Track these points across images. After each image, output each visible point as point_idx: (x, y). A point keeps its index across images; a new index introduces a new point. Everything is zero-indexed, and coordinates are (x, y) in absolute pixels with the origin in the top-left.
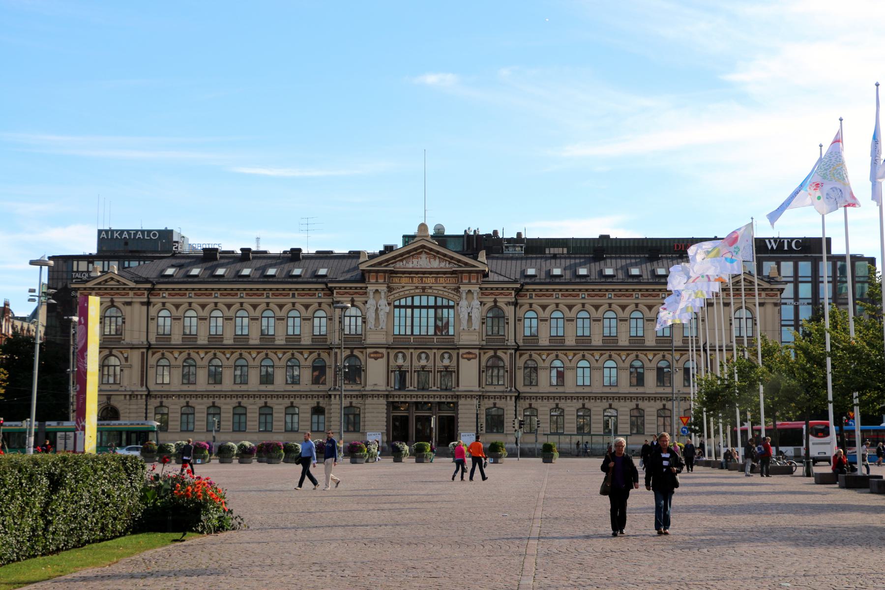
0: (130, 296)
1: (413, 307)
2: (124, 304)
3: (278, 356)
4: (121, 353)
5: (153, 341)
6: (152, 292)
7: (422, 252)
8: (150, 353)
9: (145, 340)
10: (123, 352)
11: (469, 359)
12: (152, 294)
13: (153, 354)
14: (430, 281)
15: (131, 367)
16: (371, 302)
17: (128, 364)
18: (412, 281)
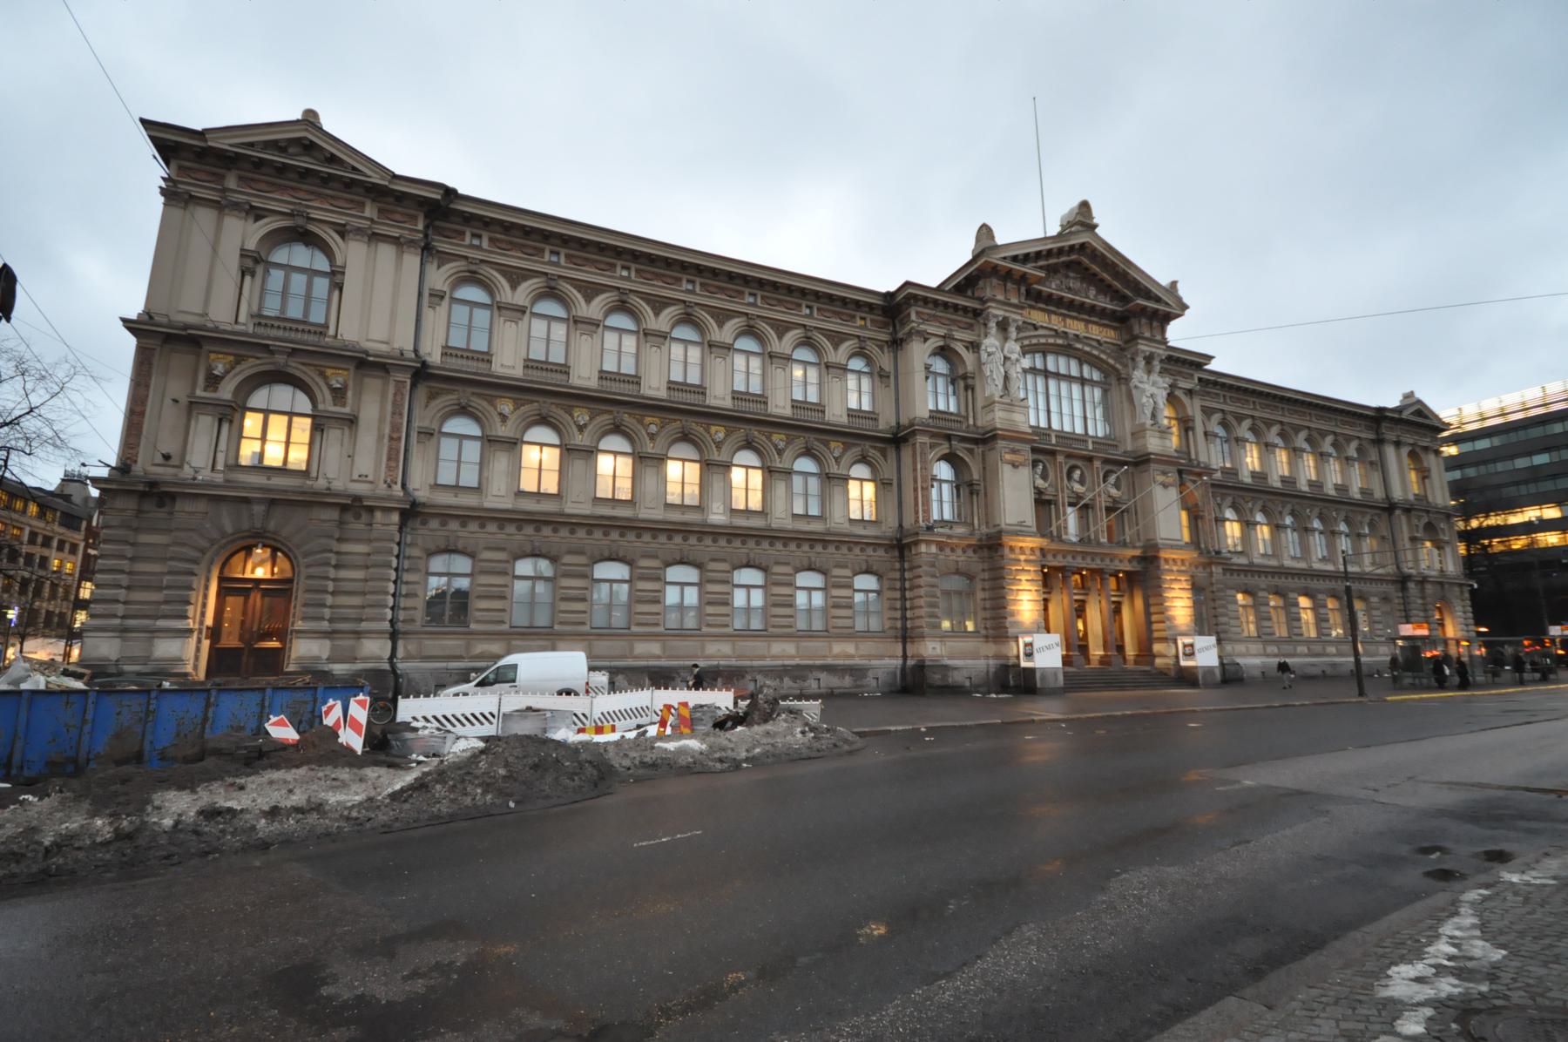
0: (367, 213)
1: (1046, 374)
2: (342, 235)
3: (776, 446)
4: (322, 374)
5: (434, 357)
6: (437, 223)
7: (1068, 266)
8: (422, 392)
9: (411, 348)
10: (329, 372)
11: (1165, 486)
12: (441, 232)
13: (432, 396)
14: (1075, 327)
15: (352, 421)
16: (991, 342)
17: (347, 410)
18: (1050, 319)
